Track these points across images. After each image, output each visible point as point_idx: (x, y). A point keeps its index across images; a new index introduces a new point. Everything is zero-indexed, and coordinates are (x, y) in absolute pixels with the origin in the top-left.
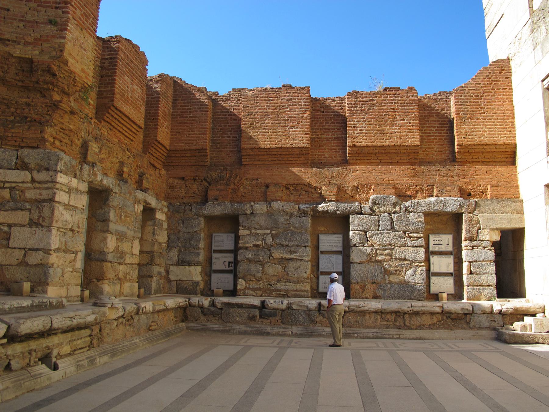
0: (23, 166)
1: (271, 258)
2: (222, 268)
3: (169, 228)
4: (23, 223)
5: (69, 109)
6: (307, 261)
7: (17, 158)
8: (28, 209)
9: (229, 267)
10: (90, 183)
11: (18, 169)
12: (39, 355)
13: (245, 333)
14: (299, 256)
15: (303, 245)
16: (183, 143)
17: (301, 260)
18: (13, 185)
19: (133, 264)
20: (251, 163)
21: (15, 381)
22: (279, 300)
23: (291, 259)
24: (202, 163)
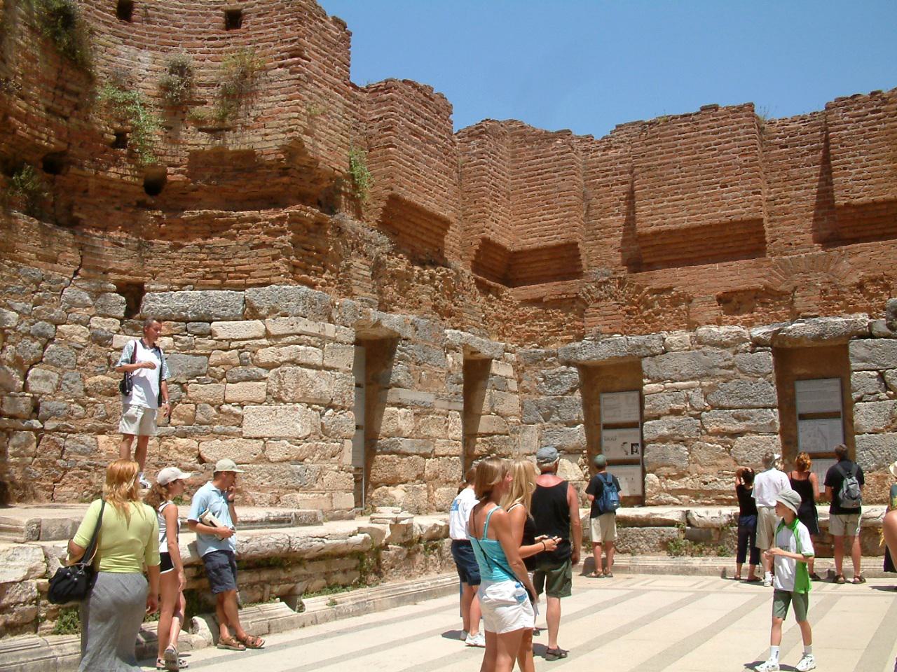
0: (252, 313)
7: (245, 302)
9: (632, 453)
11: (247, 320)
13: (654, 571)
16: (535, 237)
18: (242, 343)
19: (451, 456)
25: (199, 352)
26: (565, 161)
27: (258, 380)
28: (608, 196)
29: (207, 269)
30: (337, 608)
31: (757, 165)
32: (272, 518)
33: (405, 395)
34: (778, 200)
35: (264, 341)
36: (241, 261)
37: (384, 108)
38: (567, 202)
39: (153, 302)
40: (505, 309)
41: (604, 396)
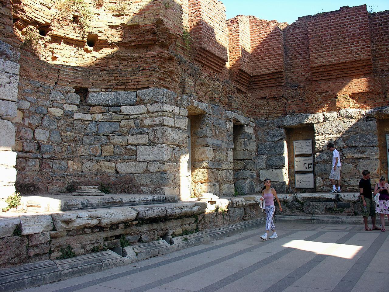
0: (141, 102)
1: (344, 158)
2: (304, 169)
3: (257, 140)
4: (144, 143)
5: (168, 56)
6: (377, 159)
7: (136, 97)
8: (147, 133)
9: (309, 168)
10: (189, 109)
11: (138, 105)
12: (161, 233)
13: (323, 222)
14: (368, 155)
15: (371, 145)
16: (262, 69)
17: (370, 159)
18: (136, 116)
19: (229, 170)
20: (320, 78)
21: (145, 249)
22: (351, 194)
23: (362, 158)
24: (280, 84)
25: (115, 121)
26: (276, 34)
27: (144, 134)
28: (295, 50)
29: (119, 81)
30: (188, 242)
31: (368, 34)
32: (155, 199)
33: (210, 141)
34: (378, 50)
35: (146, 115)
36: (134, 77)
37: (197, 7)
38: (277, 53)
39: (93, 97)
40: (248, 102)
41: (295, 142)
